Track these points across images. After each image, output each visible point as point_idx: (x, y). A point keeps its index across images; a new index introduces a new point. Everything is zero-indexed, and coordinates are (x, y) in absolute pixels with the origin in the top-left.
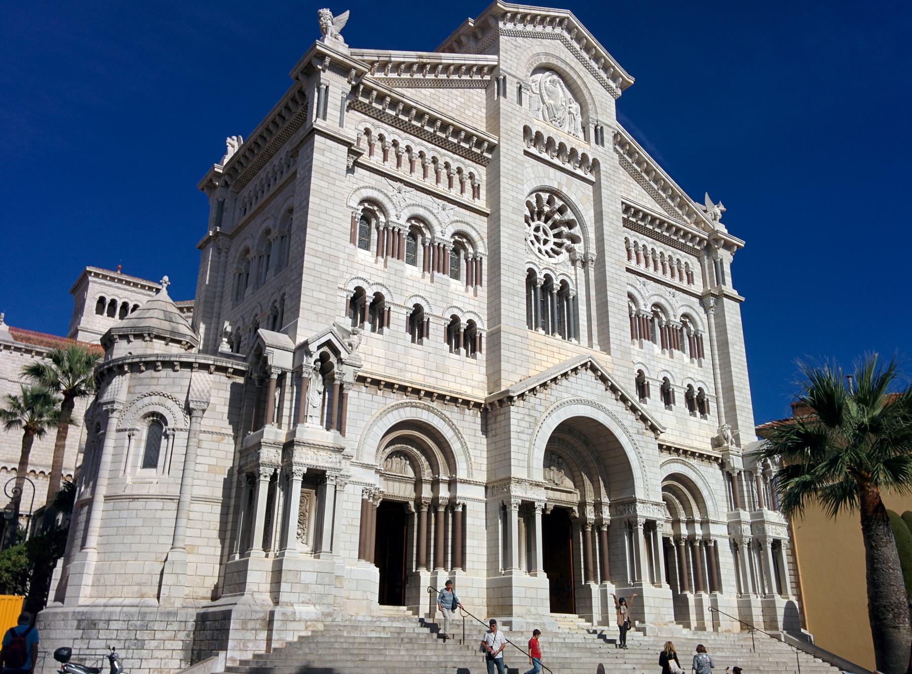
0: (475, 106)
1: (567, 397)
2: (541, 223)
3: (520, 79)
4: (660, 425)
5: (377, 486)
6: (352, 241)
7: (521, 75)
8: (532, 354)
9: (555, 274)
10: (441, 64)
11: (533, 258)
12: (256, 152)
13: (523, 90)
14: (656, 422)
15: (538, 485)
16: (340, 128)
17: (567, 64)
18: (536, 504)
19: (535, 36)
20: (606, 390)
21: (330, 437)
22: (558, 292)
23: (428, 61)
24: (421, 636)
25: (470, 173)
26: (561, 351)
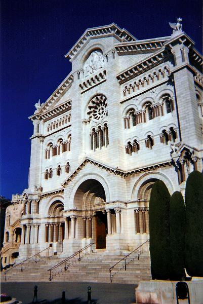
2: (101, 107)
11: (94, 124)
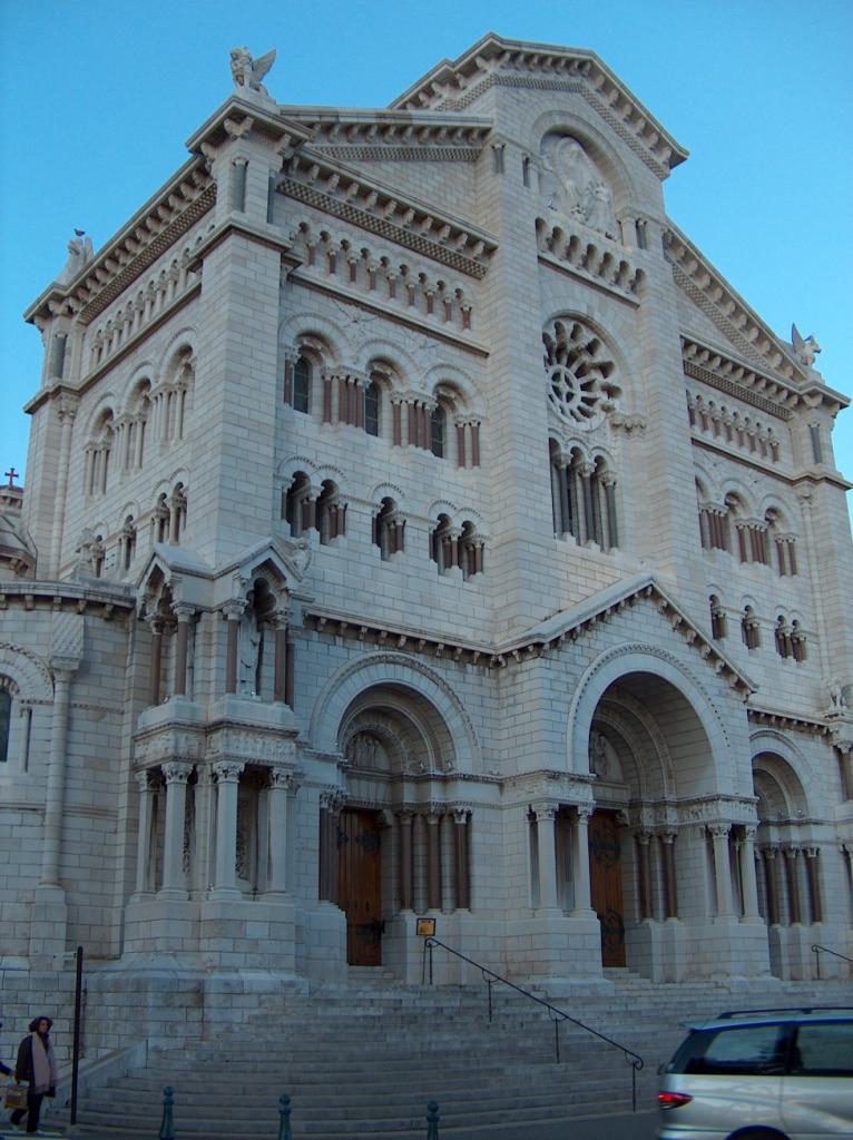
0: (460, 189)
1: (620, 643)
2: (562, 368)
3: (526, 149)
4: (750, 681)
5: (341, 789)
6: (287, 399)
7: (526, 143)
8: (563, 575)
9: (586, 447)
10: (411, 125)
12: (122, 260)
13: (530, 165)
14: (746, 677)
15: (581, 780)
16: (269, 225)
17: (591, 127)
18: (580, 809)
19: (544, 86)
20: (674, 629)
21: (272, 713)
22: (592, 475)
23: (393, 122)
24: (426, 1012)
25: (458, 291)
26: (607, 570)
